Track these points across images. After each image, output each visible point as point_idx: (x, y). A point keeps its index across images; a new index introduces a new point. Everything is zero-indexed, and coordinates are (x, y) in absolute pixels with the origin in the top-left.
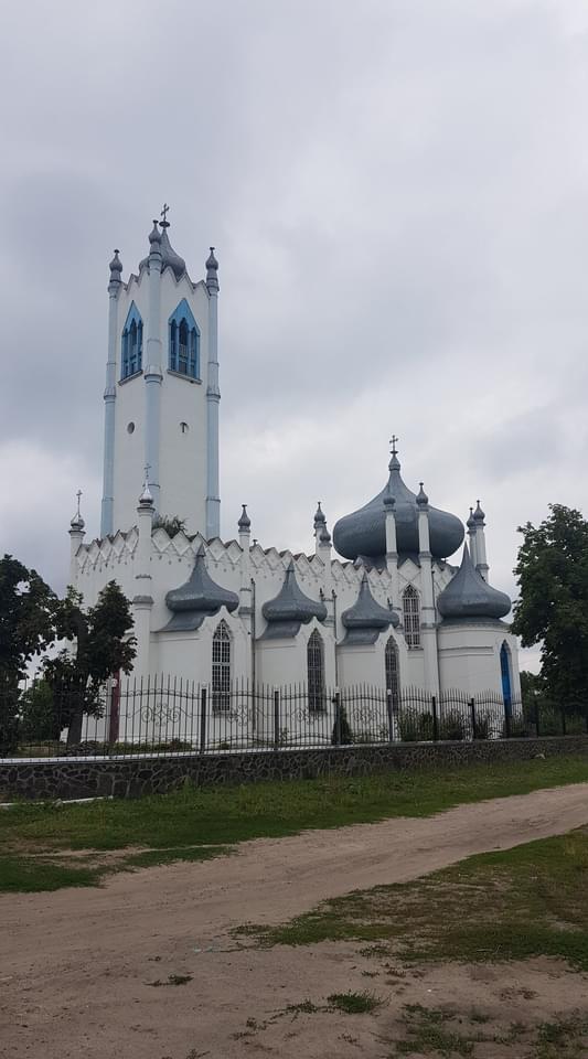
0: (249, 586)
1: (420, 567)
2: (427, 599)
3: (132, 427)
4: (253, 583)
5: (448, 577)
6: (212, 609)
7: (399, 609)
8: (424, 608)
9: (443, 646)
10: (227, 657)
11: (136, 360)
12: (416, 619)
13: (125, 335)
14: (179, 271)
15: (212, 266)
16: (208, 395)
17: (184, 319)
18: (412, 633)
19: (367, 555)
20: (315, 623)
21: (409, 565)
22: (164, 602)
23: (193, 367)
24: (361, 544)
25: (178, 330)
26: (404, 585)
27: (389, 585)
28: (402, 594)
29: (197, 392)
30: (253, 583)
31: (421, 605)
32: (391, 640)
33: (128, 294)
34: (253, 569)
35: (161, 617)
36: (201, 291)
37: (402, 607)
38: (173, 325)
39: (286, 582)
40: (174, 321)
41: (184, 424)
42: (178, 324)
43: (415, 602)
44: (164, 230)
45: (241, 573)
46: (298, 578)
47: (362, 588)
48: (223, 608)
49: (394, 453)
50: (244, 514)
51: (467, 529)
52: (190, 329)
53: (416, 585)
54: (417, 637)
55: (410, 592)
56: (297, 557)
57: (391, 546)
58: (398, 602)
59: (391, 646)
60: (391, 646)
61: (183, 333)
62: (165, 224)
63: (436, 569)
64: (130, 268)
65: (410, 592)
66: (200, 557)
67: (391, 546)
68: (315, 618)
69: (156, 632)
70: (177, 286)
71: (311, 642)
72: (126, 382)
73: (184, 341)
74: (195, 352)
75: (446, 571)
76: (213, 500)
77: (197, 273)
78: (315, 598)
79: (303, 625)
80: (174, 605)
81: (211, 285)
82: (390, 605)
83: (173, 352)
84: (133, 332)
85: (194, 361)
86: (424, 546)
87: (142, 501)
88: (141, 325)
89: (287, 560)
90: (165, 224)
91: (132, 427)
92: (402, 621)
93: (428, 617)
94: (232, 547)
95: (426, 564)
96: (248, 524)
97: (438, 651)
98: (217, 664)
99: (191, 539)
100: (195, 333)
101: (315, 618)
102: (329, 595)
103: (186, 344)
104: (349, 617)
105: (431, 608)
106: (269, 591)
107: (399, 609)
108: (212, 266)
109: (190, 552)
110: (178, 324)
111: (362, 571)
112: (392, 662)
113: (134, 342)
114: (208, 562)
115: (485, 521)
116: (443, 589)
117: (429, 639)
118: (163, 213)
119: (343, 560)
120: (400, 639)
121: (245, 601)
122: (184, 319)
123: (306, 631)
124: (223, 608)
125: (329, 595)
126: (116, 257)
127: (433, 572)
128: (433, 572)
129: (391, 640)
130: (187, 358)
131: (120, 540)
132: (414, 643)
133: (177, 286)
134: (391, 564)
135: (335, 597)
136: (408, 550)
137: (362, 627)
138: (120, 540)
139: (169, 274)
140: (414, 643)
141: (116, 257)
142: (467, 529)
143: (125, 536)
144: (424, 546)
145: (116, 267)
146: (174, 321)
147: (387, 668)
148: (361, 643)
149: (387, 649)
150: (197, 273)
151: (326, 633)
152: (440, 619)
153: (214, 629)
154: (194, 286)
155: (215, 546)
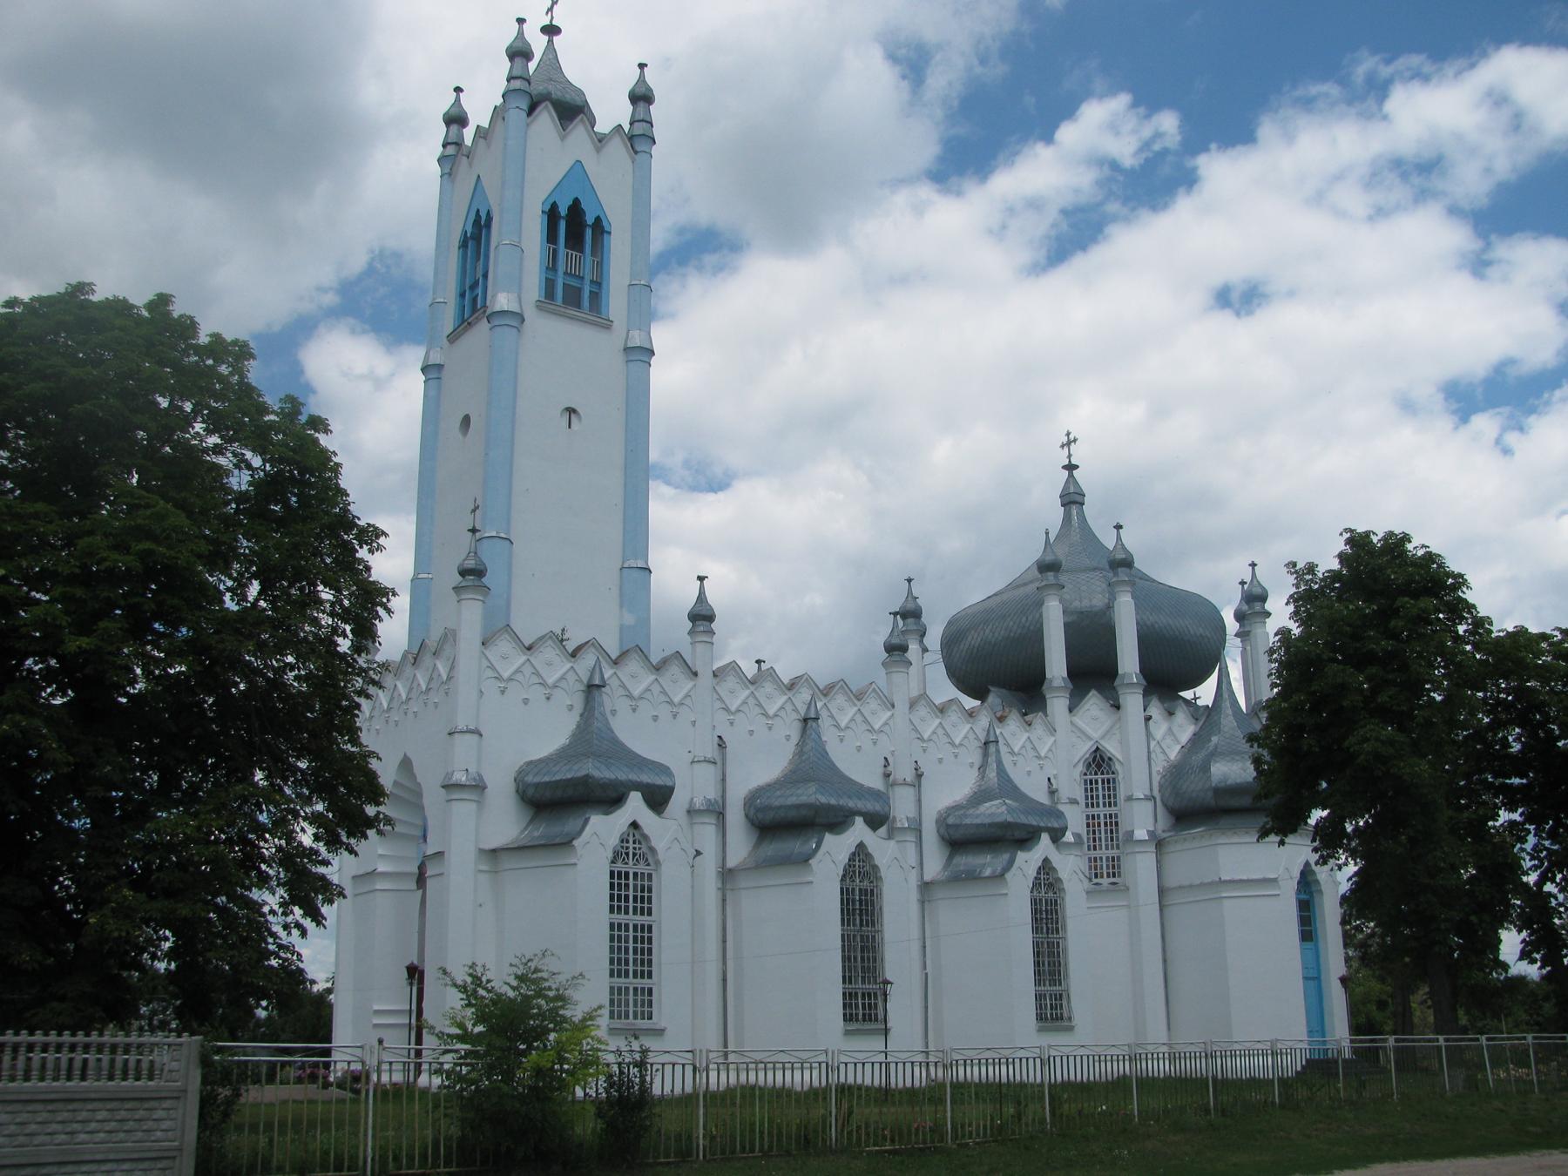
0: (710, 751)
1: (1118, 707)
2: (1138, 778)
3: (466, 421)
4: (721, 744)
5: (1185, 729)
6: (611, 799)
7: (1074, 802)
8: (1130, 798)
9: (1171, 882)
10: (644, 902)
11: (479, 291)
12: (1113, 823)
13: (464, 245)
14: (572, 110)
15: (641, 97)
16: (627, 350)
17: (576, 202)
18: (1103, 853)
19: (1018, 689)
20: (858, 831)
21: (1094, 704)
22: (511, 787)
23: (596, 297)
24: (998, 667)
25: (562, 225)
26: (1085, 749)
27: (1047, 751)
28: (1081, 768)
30: (721, 744)
31: (1122, 792)
32: (1046, 867)
33: (470, 165)
34: (764, 720)
35: (504, 821)
36: (617, 148)
37: (1082, 802)
38: (552, 214)
39: (801, 745)
40: (554, 207)
41: (571, 411)
42: (563, 211)
43: (1111, 784)
44: (550, 42)
46: (829, 735)
47: (985, 755)
48: (635, 800)
49: (1071, 467)
50: (702, 597)
51: (1231, 625)
52: (590, 220)
53: (1111, 748)
54: (1115, 863)
55: (1099, 761)
56: (827, 691)
57: (1056, 665)
58: (1071, 785)
59: (1047, 877)
60: (1047, 877)
61: (574, 227)
62: (551, 30)
63: (1156, 710)
64: (479, 113)
65: (1099, 761)
66: (592, 689)
67: (1056, 665)
68: (859, 820)
69: (494, 851)
70: (563, 138)
71: (848, 873)
72: (465, 330)
74: (600, 266)
75: (1181, 716)
77: (611, 111)
78: (873, 781)
79: (828, 837)
80: (531, 792)
81: (638, 137)
82: (1052, 792)
83: (551, 266)
84: (476, 237)
85: (598, 283)
86: (1129, 661)
87: (464, 573)
89: (804, 696)
90: (551, 30)
91: (466, 421)
92: (1076, 821)
93: (1142, 820)
94: (675, 670)
95: (1133, 701)
96: (710, 618)
97: (1162, 891)
98: (621, 918)
99: (574, 655)
100: (600, 228)
101: (859, 820)
102: (904, 772)
103: (581, 250)
104: (951, 821)
105: (1147, 798)
106: (761, 764)
107: (1074, 802)
108: (641, 97)
109: (571, 677)
110: (563, 211)
111: (984, 720)
112: (1047, 916)
114: (611, 700)
115: (1268, 606)
116: (1174, 753)
117: (1141, 868)
118: (550, 10)
119: (970, 703)
120: (1070, 867)
121: (693, 785)
122: (576, 202)
123: (836, 849)
124: (635, 800)
125: (904, 772)
126: (458, 100)
127: (1148, 719)
128: (1148, 719)
129: (1046, 867)
130: (582, 278)
132: (1107, 875)
133: (563, 138)
134: (1057, 704)
135: (919, 776)
136: (1093, 672)
137: (984, 839)
139: (546, 119)
140: (1107, 875)
141: (458, 100)
142: (1231, 625)
144: (1129, 661)
145: (456, 119)
146: (554, 207)
147: (1036, 930)
148: (972, 877)
149: (1036, 884)
150: (611, 111)
151: (882, 849)
152: (1164, 821)
153: (614, 841)
154: (601, 140)
155: (633, 665)
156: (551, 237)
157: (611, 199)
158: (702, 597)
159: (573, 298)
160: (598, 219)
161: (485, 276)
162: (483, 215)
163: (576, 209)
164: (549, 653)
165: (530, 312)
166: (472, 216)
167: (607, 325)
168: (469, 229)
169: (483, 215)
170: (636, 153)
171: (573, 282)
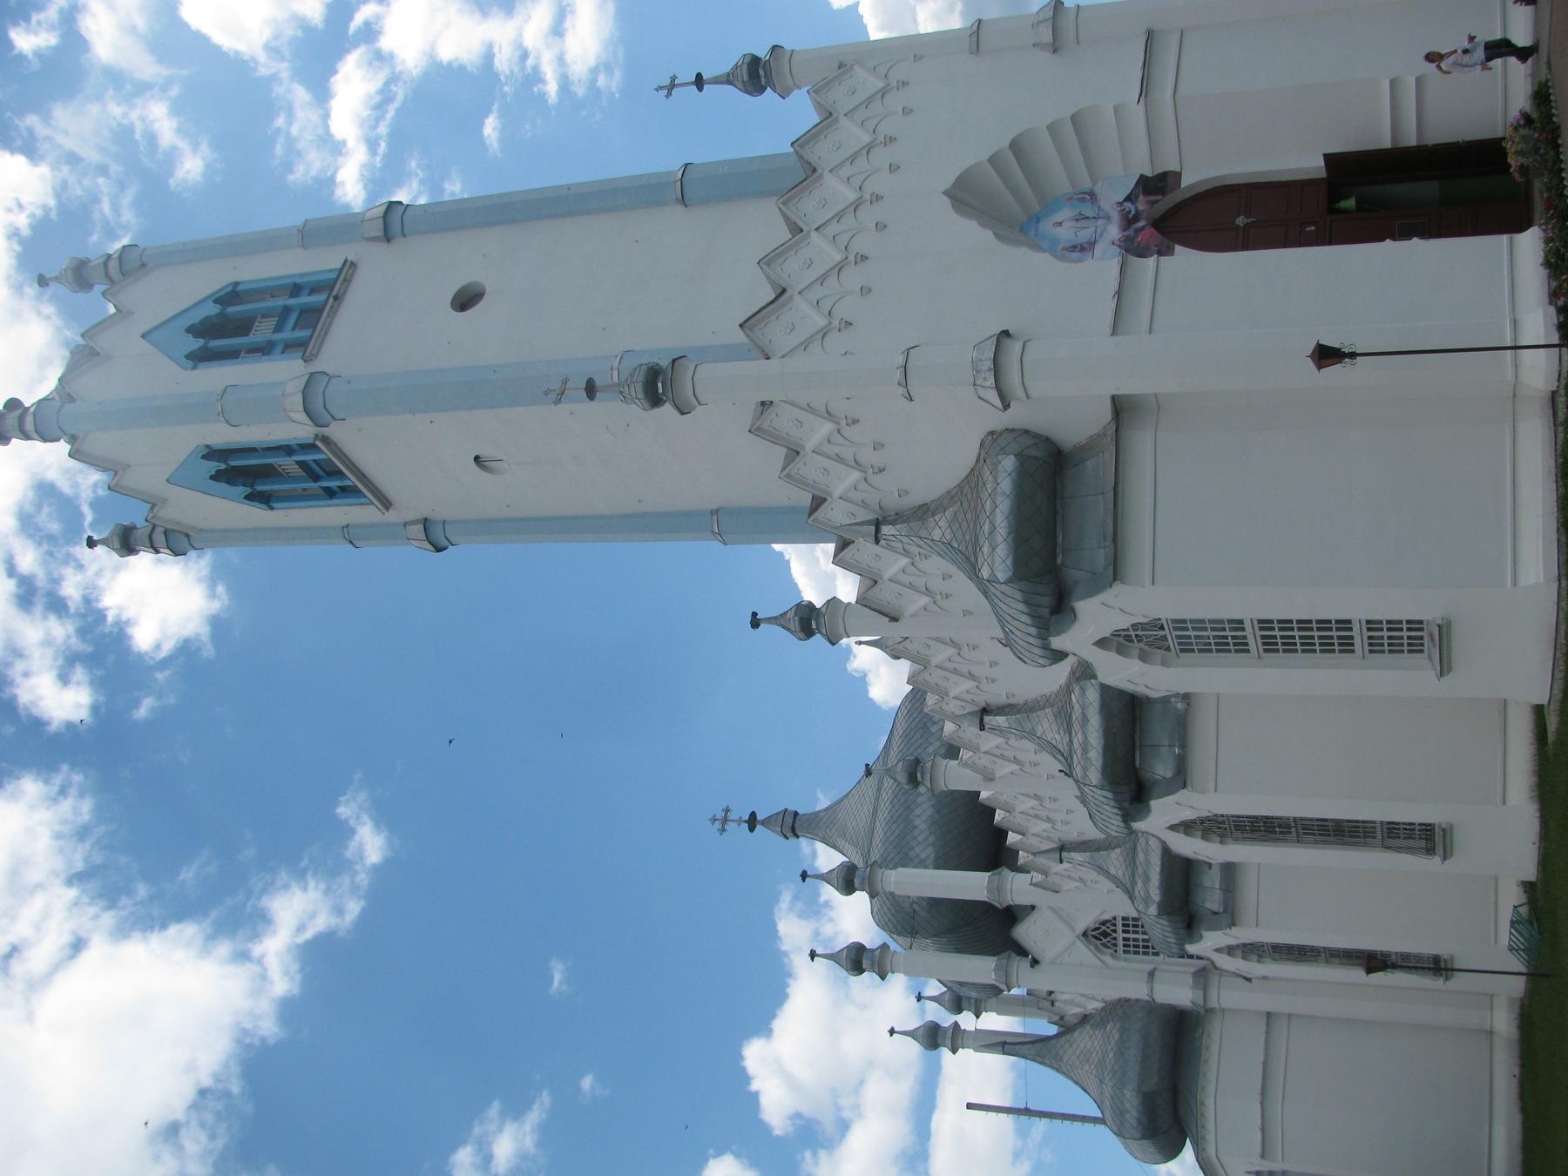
13: (265, 499)
17: (188, 330)
29: (379, 270)
42: (196, 344)
45: (917, 58)
50: (728, 79)
52: (212, 310)
61: (224, 330)
73: (243, 326)
76: (686, 189)
83: (265, 350)
85: (296, 290)
88: (212, 454)
110: (200, 343)
113: (268, 472)
122: (188, 330)
130: (287, 310)
131: (810, 467)
138: (810, 467)
143: (794, 453)
156: (231, 355)
157: (192, 289)
158: (728, 79)
159: (312, 317)
160: (215, 301)
161: (287, 450)
162: (214, 466)
163: (193, 330)
164: (792, 270)
165: (316, 366)
166: (224, 486)
167: (349, 269)
168: (242, 490)
169: (214, 466)
170: (143, 265)
171: (293, 318)
